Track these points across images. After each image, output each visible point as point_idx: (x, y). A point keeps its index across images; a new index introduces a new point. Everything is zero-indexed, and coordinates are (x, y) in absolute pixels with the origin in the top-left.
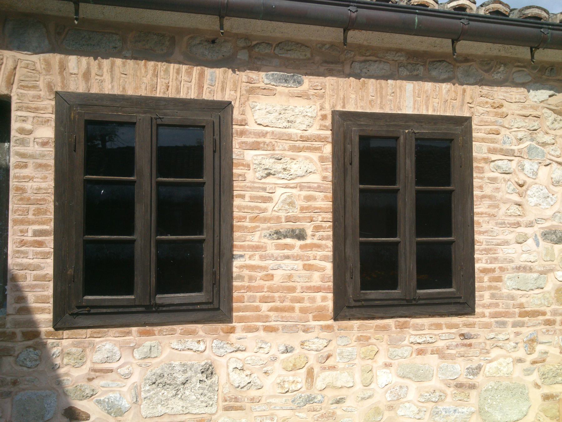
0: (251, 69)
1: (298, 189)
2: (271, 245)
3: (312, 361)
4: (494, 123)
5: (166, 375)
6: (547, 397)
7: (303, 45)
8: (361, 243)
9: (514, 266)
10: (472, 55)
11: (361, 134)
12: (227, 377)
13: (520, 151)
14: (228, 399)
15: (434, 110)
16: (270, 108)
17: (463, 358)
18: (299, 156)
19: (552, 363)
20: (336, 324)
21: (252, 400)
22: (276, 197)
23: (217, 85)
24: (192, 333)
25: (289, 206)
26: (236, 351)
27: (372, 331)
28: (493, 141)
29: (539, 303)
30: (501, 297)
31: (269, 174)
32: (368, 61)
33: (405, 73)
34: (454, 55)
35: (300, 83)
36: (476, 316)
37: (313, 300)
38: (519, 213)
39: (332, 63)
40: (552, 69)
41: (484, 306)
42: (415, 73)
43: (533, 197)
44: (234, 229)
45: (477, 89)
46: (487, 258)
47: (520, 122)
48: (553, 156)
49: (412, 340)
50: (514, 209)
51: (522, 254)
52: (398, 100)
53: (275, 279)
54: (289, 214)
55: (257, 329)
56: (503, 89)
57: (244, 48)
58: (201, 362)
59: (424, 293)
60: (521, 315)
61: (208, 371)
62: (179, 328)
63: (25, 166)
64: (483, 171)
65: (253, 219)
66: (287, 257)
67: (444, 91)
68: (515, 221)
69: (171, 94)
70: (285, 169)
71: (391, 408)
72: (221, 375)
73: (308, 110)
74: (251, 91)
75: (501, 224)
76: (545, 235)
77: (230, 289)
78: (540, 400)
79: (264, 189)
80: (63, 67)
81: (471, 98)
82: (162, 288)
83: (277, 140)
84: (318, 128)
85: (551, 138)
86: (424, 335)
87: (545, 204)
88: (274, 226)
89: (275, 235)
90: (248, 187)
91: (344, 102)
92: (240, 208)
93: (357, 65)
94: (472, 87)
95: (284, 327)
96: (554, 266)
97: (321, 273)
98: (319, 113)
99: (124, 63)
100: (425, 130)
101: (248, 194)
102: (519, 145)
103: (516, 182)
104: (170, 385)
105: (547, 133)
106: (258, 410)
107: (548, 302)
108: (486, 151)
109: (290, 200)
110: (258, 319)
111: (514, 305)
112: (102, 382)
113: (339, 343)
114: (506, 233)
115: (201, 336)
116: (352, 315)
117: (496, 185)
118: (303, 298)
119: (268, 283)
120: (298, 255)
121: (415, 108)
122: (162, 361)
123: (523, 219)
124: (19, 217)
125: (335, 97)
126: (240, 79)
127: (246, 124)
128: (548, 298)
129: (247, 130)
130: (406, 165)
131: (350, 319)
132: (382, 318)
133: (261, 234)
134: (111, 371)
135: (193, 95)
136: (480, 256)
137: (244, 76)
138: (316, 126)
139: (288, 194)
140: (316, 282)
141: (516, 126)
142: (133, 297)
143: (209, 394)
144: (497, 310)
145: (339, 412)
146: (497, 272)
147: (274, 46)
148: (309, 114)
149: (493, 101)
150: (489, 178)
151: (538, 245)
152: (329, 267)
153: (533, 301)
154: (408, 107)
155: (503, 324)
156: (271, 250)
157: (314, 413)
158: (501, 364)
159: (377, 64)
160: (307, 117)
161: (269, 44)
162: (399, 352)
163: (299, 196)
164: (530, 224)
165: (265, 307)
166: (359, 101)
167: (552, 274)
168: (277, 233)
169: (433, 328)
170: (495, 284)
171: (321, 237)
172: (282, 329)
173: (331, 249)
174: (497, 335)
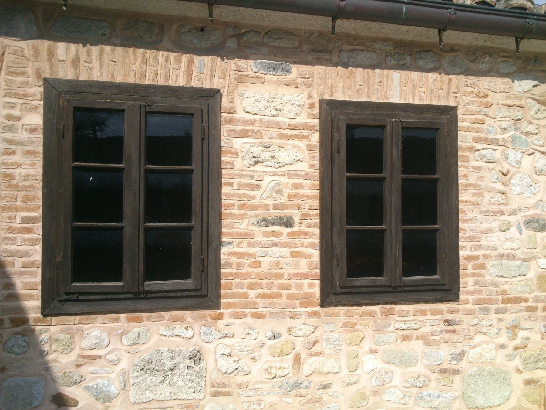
0: (240, 57)
1: (286, 177)
2: (258, 232)
3: (299, 348)
4: (479, 113)
5: (154, 361)
6: (528, 382)
7: (291, 33)
8: (348, 231)
9: (498, 254)
10: (458, 45)
11: (350, 122)
12: (215, 362)
13: (504, 140)
14: (216, 384)
15: (420, 100)
16: (259, 97)
17: (447, 344)
18: (287, 144)
19: (534, 348)
20: (323, 311)
21: (240, 386)
22: (264, 184)
23: (205, 72)
24: (181, 319)
25: (277, 194)
26: (224, 337)
27: (358, 317)
28: (478, 130)
29: (522, 289)
30: (485, 284)
31: (257, 162)
32: (356, 50)
33: (393, 62)
34: (441, 45)
35: (288, 71)
36: (460, 303)
37: (300, 287)
38: (503, 202)
39: (320, 52)
40: (536, 60)
41: (467, 293)
42: (402, 62)
43: (516, 187)
44: (223, 217)
46: (471, 245)
47: (505, 112)
48: (536, 145)
49: (397, 326)
50: (498, 198)
51: (505, 241)
52: (385, 90)
53: (262, 266)
54: (276, 202)
55: (245, 316)
56: (489, 79)
57: (233, 36)
58: (189, 348)
59: (410, 280)
60: (504, 302)
61: (196, 357)
62: (167, 315)
63: (14, 153)
64: (468, 159)
65: (242, 207)
66: (275, 245)
67: (430, 81)
68: (499, 210)
69: (160, 81)
70: (273, 157)
71: (376, 393)
72: (209, 361)
73: (296, 99)
74: (240, 79)
75: (485, 212)
76: (528, 223)
77: (218, 276)
78: (522, 385)
79: (252, 177)
80: (51, 54)
81: (457, 88)
82: (150, 275)
83: (265, 128)
84: (306, 117)
85: (535, 127)
86: (409, 321)
87: (528, 193)
88: (262, 214)
89: (263, 223)
90: (236, 175)
91: (331, 91)
92: (228, 195)
93: (344, 54)
94: (458, 77)
95: (271, 314)
96: (536, 254)
97: (308, 260)
98: (308, 102)
99: (112, 50)
100: (412, 119)
101: (236, 182)
102: (503, 134)
103: (500, 171)
104: (158, 371)
105: (531, 123)
106: (245, 395)
107: (531, 289)
108: (471, 140)
109: (278, 188)
110: (246, 305)
111: (497, 292)
112: (91, 369)
113: (326, 329)
114: (490, 221)
115: (189, 323)
116: (338, 302)
117: (480, 174)
118: (291, 285)
119: (255, 270)
120: (285, 242)
121: (401, 97)
122: (150, 348)
123: (507, 208)
124: (7, 203)
125: (323, 86)
126: (229, 67)
127: (235, 112)
128: (530, 285)
129: (235, 118)
130: (393, 154)
131: (336, 306)
132: (368, 304)
133: (249, 221)
134: (100, 357)
135: (181, 83)
136: (464, 244)
137: (232, 64)
138: (304, 114)
139: (275, 182)
140: (304, 269)
141: (501, 115)
142: (121, 284)
143: (197, 380)
144: (481, 296)
145: (325, 398)
146: (480, 260)
147: (262, 34)
148: (297, 103)
149: (478, 90)
150: (473, 167)
151: (521, 233)
152: (316, 254)
153: (515, 288)
154: (395, 97)
155: (486, 311)
156: (259, 238)
157: (301, 398)
159: (364, 53)
160: (295, 106)
161: (257, 32)
162: (385, 338)
163: (287, 183)
164: (513, 212)
165: (252, 293)
166: (346, 90)
167: (534, 262)
168: (265, 220)
169: (418, 314)
170: (478, 271)
171: (308, 225)
172: (270, 316)
173: (318, 236)
174: (480, 321)
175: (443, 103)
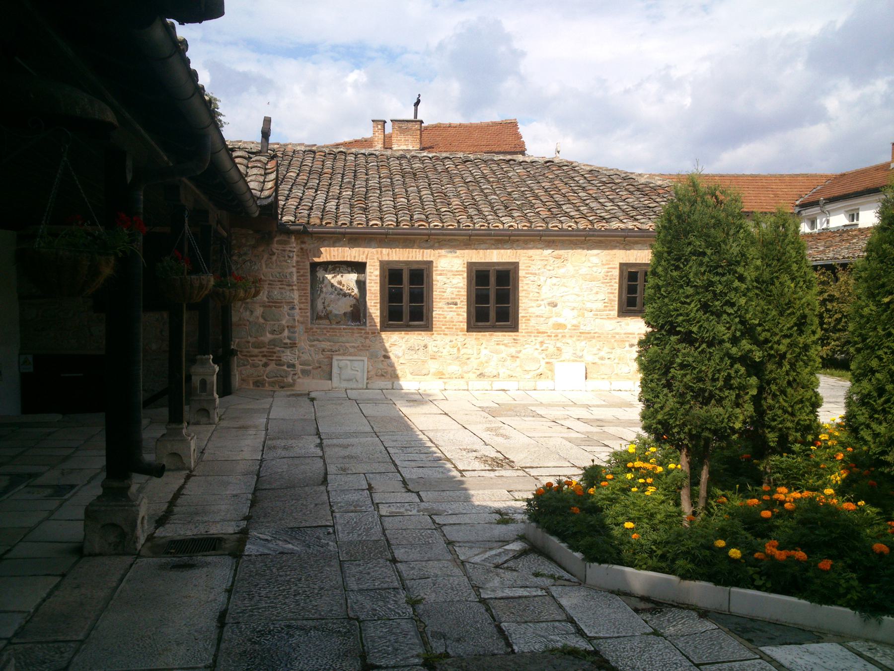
2: (446, 306)
6: (547, 363)
12: (431, 348)
43: (545, 289)
47: (539, 262)
58: (422, 343)
61: (426, 346)
69: (414, 259)
76: (549, 304)
100: (500, 268)
130: (493, 279)
135: (420, 259)
137: (437, 251)
152: (465, 315)
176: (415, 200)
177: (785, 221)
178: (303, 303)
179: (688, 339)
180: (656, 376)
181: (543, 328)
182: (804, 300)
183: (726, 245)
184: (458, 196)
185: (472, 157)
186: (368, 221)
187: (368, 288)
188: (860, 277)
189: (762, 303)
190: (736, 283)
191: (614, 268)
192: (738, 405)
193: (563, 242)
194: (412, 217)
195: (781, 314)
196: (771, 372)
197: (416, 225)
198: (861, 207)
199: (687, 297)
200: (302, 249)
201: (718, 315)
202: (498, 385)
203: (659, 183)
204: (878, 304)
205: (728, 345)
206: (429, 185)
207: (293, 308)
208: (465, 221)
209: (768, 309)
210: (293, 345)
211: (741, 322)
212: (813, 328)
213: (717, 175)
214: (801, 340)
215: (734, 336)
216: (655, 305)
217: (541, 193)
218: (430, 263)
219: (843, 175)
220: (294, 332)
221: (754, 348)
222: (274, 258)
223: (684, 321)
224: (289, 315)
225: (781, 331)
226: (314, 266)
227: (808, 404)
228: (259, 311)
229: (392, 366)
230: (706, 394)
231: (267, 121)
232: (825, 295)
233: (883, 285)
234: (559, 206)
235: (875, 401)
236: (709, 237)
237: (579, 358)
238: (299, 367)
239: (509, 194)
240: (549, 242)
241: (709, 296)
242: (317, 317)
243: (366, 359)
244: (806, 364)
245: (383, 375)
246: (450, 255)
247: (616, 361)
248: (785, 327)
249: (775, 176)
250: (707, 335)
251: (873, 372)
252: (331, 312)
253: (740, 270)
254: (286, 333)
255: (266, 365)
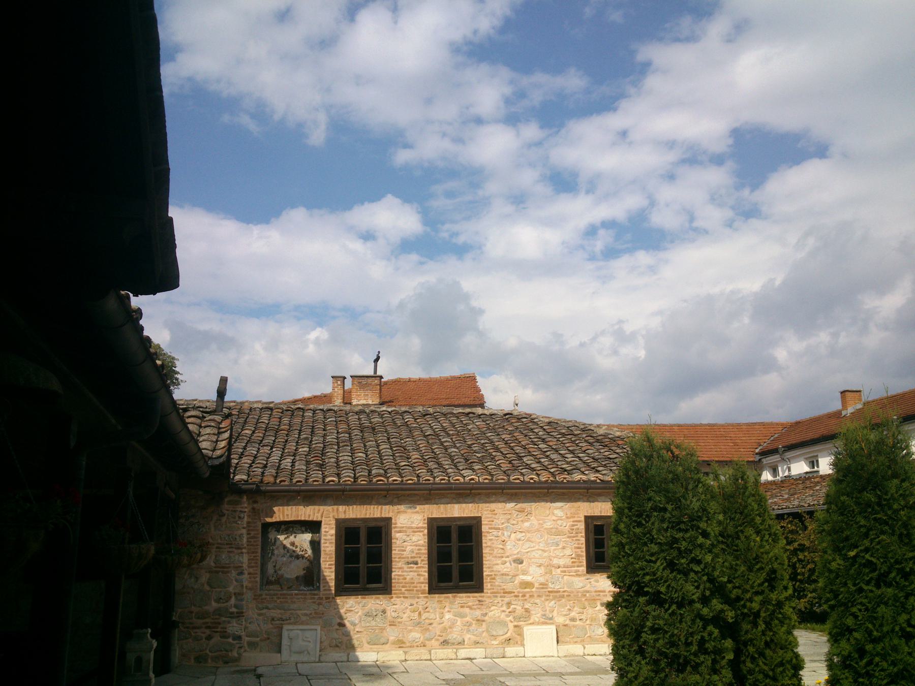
2: (405, 567)
6: (515, 626)
12: (390, 613)
43: (509, 546)
45: (484, 505)
50: (501, 551)
61: (384, 612)
69: (372, 516)
71: (450, 628)
72: (388, 613)
76: (515, 561)
80: (338, 510)
82: (368, 583)
130: (454, 536)
135: (379, 516)
137: (396, 507)
154: (456, 514)
156: (406, 569)
158: (496, 612)
175: (476, 515)
176: (374, 455)
177: (744, 473)
178: (252, 567)
179: (657, 599)
180: (627, 642)
181: (509, 587)
182: (771, 554)
183: (686, 500)
184: (418, 449)
185: (431, 410)
186: (324, 477)
187: (322, 549)
188: (824, 530)
189: (730, 558)
190: (701, 540)
191: (579, 521)
192: (715, 671)
193: (525, 495)
194: (370, 471)
195: (750, 569)
196: (747, 632)
197: (375, 480)
198: (819, 454)
199: (652, 555)
200: (253, 509)
201: (686, 574)
202: (463, 653)
203: (618, 434)
204: (845, 558)
205: (698, 605)
206: (388, 439)
207: (242, 573)
208: (426, 477)
209: (737, 565)
210: (240, 615)
211: (709, 580)
212: (785, 583)
213: (675, 425)
214: (773, 596)
215: (703, 595)
216: (620, 564)
217: (501, 445)
218: (389, 520)
219: (798, 423)
220: (242, 600)
221: (726, 607)
222: (224, 519)
223: (651, 580)
224: (236, 580)
225: (752, 587)
226: (266, 527)
227: (789, 666)
228: (204, 577)
229: (347, 635)
230: (681, 661)
231: (224, 381)
232: (796, 545)
233: (847, 539)
234: (520, 458)
235: (857, 663)
236: (668, 492)
237: (547, 620)
238: (247, 639)
239: (470, 446)
240: (512, 495)
241: (675, 553)
242: (267, 582)
243: (319, 628)
244: (782, 623)
245: (337, 646)
246: (409, 510)
247: (588, 622)
248: (756, 584)
249: (732, 425)
250: (676, 595)
251: (850, 631)
252: (282, 576)
253: (703, 525)
254: (233, 601)
255: (209, 638)
